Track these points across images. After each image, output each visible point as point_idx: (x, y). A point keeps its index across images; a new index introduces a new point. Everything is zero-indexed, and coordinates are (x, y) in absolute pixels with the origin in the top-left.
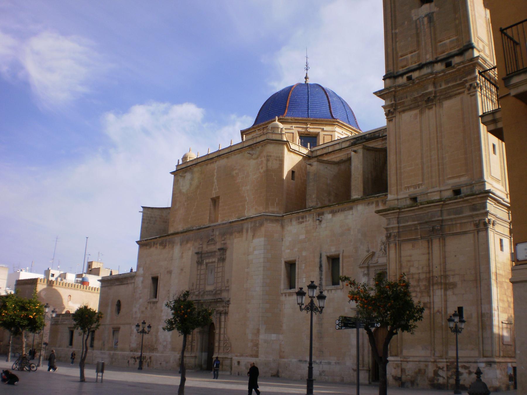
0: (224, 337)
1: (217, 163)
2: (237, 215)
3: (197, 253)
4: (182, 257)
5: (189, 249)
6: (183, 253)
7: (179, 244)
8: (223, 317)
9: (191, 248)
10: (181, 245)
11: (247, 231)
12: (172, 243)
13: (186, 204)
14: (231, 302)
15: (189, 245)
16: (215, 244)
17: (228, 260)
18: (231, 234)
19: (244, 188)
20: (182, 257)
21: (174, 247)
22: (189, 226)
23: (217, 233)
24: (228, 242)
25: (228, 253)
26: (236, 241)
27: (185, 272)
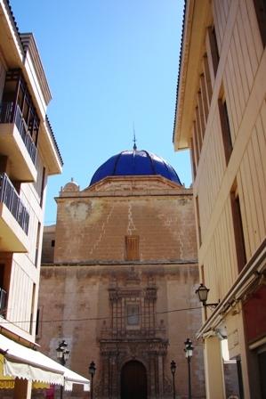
0: (164, 379)
1: (132, 202)
2: (169, 258)
3: (110, 290)
4: (81, 291)
5: (95, 284)
6: (82, 287)
7: (75, 277)
8: (160, 359)
9: (98, 284)
10: (78, 277)
11: (186, 275)
12: (64, 275)
13: (83, 235)
14: (170, 342)
15: (93, 280)
16: (138, 284)
17: (159, 301)
18: (162, 275)
19: (175, 233)
20: (81, 291)
21: (67, 279)
22: (92, 259)
23: (140, 272)
24: (158, 283)
25: (159, 294)
26: (169, 282)
27: (89, 308)
